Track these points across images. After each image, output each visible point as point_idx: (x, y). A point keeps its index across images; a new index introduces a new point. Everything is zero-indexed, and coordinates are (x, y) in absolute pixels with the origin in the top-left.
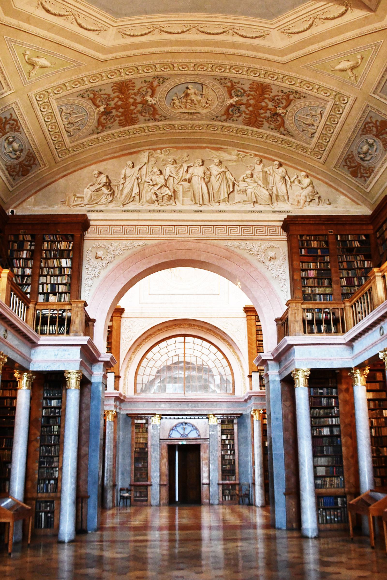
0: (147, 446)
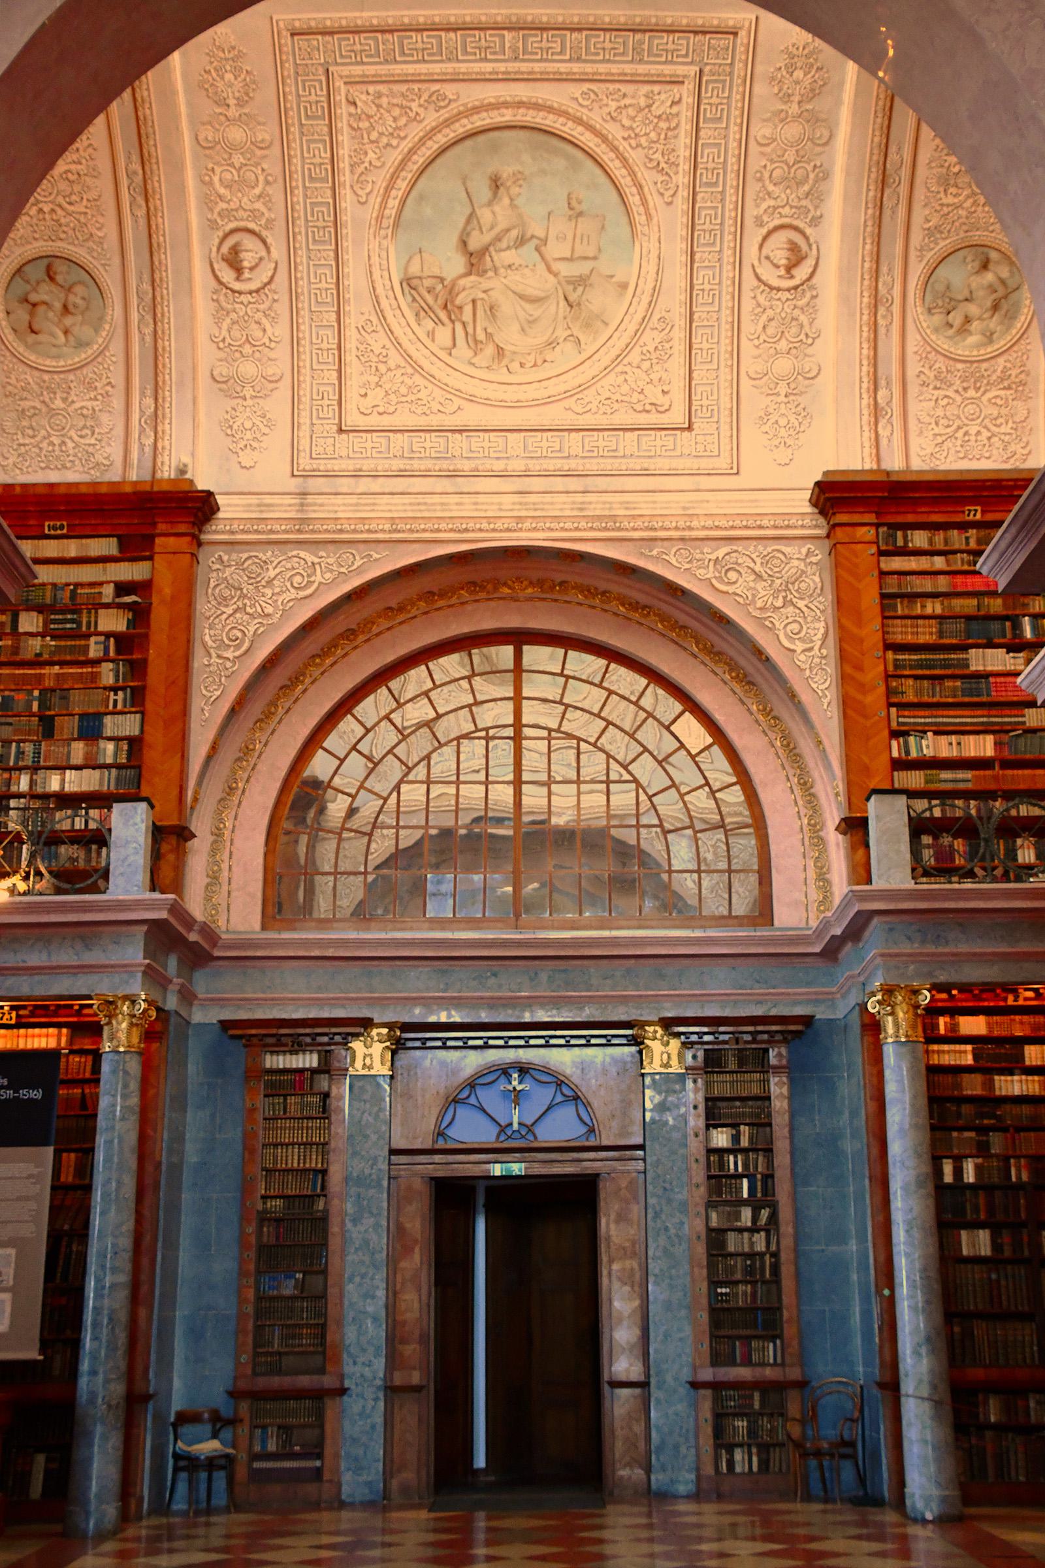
0: (323, 1188)
